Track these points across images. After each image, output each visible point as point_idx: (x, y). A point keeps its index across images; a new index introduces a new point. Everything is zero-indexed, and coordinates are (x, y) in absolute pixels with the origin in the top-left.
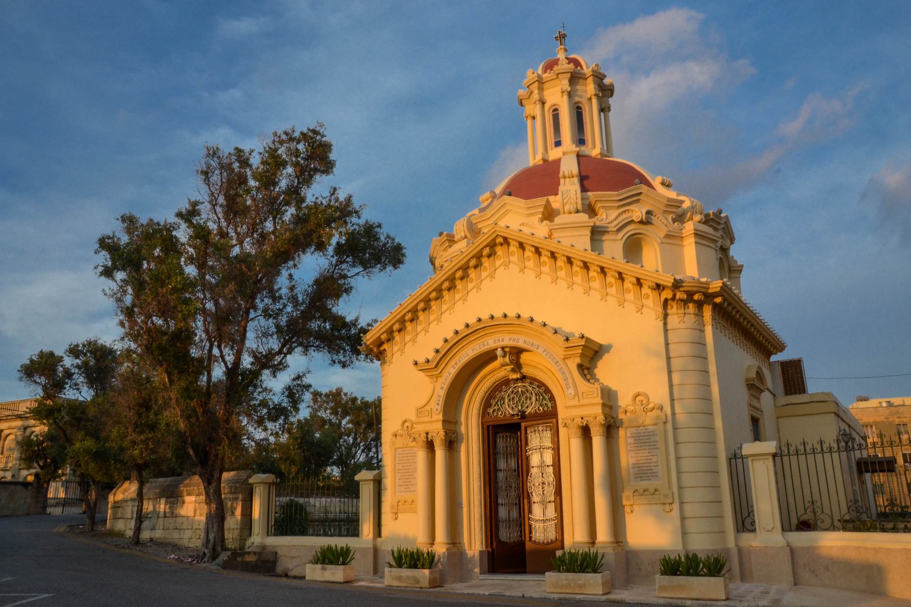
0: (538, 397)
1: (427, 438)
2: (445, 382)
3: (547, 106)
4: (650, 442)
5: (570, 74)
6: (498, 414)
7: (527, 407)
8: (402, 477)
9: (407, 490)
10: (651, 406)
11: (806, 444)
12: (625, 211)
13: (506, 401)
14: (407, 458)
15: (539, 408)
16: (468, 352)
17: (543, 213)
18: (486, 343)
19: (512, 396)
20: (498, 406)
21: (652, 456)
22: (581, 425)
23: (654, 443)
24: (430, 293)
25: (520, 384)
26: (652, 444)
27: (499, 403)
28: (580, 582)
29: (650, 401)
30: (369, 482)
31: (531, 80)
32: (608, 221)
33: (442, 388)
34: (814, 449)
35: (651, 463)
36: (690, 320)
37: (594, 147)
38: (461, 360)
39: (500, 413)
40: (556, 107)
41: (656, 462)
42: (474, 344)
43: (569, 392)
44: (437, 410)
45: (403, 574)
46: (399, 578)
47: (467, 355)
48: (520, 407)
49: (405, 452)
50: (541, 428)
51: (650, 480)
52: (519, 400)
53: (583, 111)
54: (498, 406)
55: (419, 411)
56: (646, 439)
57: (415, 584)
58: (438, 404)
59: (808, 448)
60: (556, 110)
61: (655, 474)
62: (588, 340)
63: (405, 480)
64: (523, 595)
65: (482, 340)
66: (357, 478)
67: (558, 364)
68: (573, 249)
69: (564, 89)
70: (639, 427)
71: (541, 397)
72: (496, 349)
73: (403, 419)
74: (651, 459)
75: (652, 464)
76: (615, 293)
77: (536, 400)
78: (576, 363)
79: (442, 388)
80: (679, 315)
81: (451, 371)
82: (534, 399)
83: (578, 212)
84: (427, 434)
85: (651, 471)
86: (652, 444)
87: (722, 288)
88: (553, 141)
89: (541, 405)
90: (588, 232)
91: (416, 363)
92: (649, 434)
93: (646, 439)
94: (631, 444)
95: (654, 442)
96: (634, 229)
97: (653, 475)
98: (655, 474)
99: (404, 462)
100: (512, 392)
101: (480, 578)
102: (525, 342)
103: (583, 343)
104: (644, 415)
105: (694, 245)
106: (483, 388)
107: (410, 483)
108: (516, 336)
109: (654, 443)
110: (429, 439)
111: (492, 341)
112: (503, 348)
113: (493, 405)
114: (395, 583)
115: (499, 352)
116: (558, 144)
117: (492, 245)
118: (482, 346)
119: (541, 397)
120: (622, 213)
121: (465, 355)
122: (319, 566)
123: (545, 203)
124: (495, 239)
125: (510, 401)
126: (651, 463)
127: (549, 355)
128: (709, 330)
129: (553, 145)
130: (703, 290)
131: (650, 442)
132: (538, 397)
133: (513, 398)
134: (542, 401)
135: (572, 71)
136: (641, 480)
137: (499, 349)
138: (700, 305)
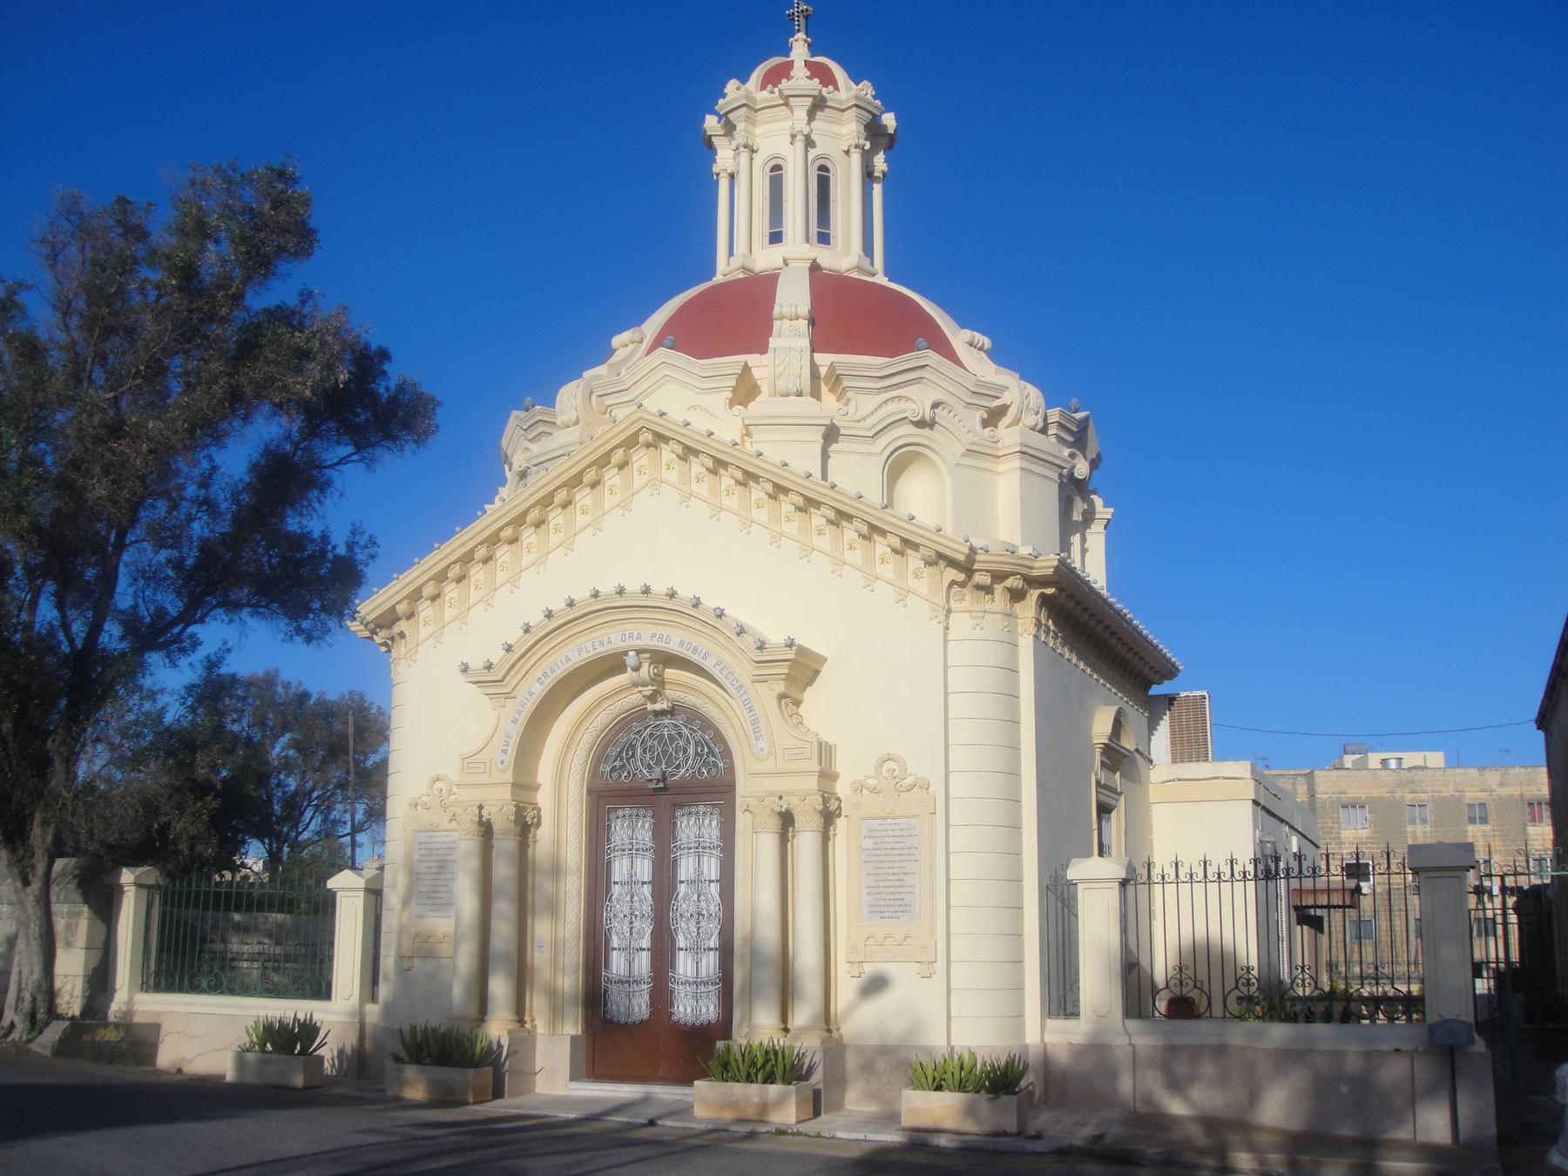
1: (481, 816)
2: (521, 708)
3: (759, 159)
5: (811, 99)
6: (620, 776)
7: (678, 767)
10: (910, 780)
11: (1180, 864)
12: (892, 399)
16: (569, 654)
17: (735, 390)
18: (605, 639)
19: (649, 744)
21: (905, 874)
22: (777, 809)
23: (913, 851)
24: (501, 529)
25: (667, 721)
26: (906, 851)
29: (909, 772)
31: (734, 100)
32: (858, 417)
33: (515, 721)
36: (994, 623)
37: (847, 251)
38: (555, 668)
39: (625, 774)
40: (779, 162)
41: (911, 886)
42: (586, 638)
43: (759, 747)
44: (502, 762)
47: (568, 660)
48: (664, 766)
51: (898, 918)
52: (664, 752)
53: (831, 175)
54: (622, 760)
55: (468, 761)
58: (505, 752)
60: (777, 168)
61: (909, 908)
62: (802, 651)
66: (332, 883)
67: (741, 692)
68: (785, 471)
69: (798, 128)
70: (885, 818)
71: (706, 750)
72: (626, 653)
75: (904, 890)
77: (697, 754)
78: (777, 692)
79: (515, 721)
80: (974, 614)
81: (534, 688)
82: (691, 751)
83: (800, 394)
84: (481, 808)
86: (906, 851)
87: (1056, 568)
88: (767, 231)
89: (705, 764)
90: (817, 436)
91: (465, 669)
92: (903, 833)
94: (868, 849)
95: (909, 848)
96: (908, 435)
97: (904, 909)
98: (909, 908)
100: (651, 735)
102: (682, 644)
103: (792, 657)
104: (896, 797)
105: (1016, 476)
106: (595, 724)
107: (441, 901)
108: (665, 631)
109: (913, 851)
110: (484, 819)
112: (639, 652)
113: (613, 758)
115: (631, 659)
116: (776, 238)
117: (631, 442)
119: (706, 750)
120: (886, 402)
121: (563, 659)
123: (739, 372)
124: (636, 434)
125: (645, 752)
126: (901, 887)
127: (726, 672)
128: (1026, 644)
129: (767, 239)
130: (1024, 571)
134: (708, 756)
135: (816, 93)
136: (882, 918)
137: (631, 654)
138: (1017, 596)
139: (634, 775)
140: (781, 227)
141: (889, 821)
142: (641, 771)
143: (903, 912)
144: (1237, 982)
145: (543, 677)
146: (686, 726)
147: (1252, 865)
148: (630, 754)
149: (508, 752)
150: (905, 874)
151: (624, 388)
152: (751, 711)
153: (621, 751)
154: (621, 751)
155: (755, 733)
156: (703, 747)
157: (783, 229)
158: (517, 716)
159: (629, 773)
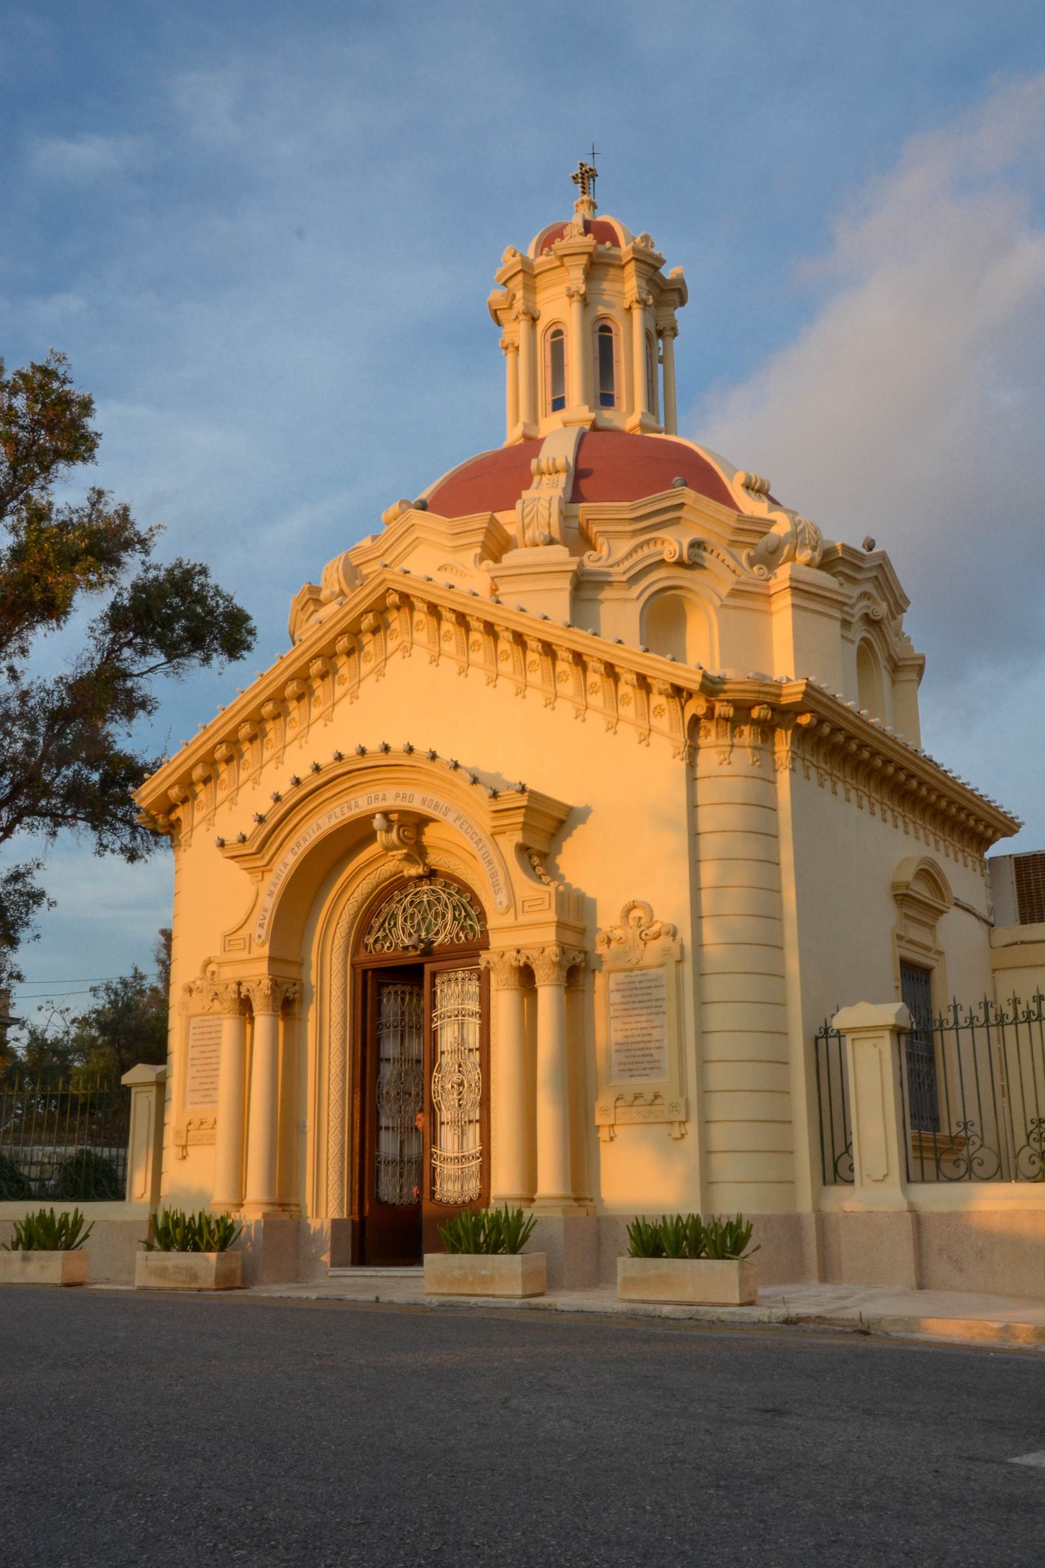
0: (457, 913)
1: (240, 993)
2: (276, 881)
3: (541, 325)
4: (650, 1001)
5: (586, 257)
6: (383, 947)
7: (437, 933)
8: (200, 1074)
9: (206, 1099)
10: (655, 928)
12: (648, 542)
13: (400, 920)
14: (209, 1036)
15: (458, 934)
16: (320, 822)
17: (484, 546)
18: (353, 803)
19: (410, 911)
20: (384, 930)
21: (653, 1027)
22: (515, 964)
23: (659, 1003)
24: (262, 705)
25: (426, 888)
26: (654, 1004)
27: (387, 924)
28: (484, 1272)
29: (655, 919)
30: (148, 1088)
32: (611, 562)
33: (270, 894)
34: (972, 1018)
35: (650, 1042)
36: (743, 758)
37: (631, 409)
38: (307, 837)
39: (388, 944)
40: (560, 327)
41: (659, 1041)
42: (333, 806)
43: (498, 900)
44: (260, 937)
45: (170, 1264)
46: (162, 1272)
47: (319, 827)
48: (423, 934)
49: (207, 1023)
50: (460, 975)
51: (647, 1075)
52: (424, 919)
53: (613, 335)
54: (384, 930)
55: (229, 939)
56: (644, 995)
57: (190, 1283)
58: (261, 926)
59: (962, 1016)
60: (558, 333)
61: (657, 1064)
62: (534, 796)
63: (204, 1080)
64: (377, 1298)
65: (345, 799)
66: (126, 1079)
67: (481, 845)
68: (522, 616)
69: (574, 289)
70: (631, 970)
71: (463, 914)
72: (373, 816)
73: (203, 958)
74: (650, 1035)
75: (652, 1045)
76: (602, 705)
77: (455, 918)
78: (514, 844)
79: (270, 894)
80: (719, 749)
81: (289, 860)
82: (449, 916)
83: (551, 542)
84: (239, 984)
85: (648, 1059)
86: (654, 1004)
87: (805, 693)
88: (550, 399)
89: (462, 928)
90: (565, 584)
91: (222, 844)
92: (649, 984)
93: (644, 995)
94: (616, 1004)
95: (657, 1000)
96: (667, 578)
97: (652, 1065)
98: (657, 1064)
99: (203, 1043)
100: (412, 902)
101: (330, 1273)
102: (424, 801)
103: (525, 803)
104: (642, 946)
105: (788, 613)
106: (356, 894)
108: (408, 790)
109: (659, 1003)
110: (242, 995)
111: (365, 798)
112: (386, 814)
113: (375, 929)
114: (154, 1282)
115: (378, 822)
116: (559, 404)
117: (380, 610)
118: (345, 809)
119: (463, 914)
120: (640, 546)
121: (315, 827)
122: (19, 1253)
123: (486, 525)
124: (383, 597)
125: (405, 920)
126: (650, 1042)
127: (465, 826)
128: (784, 777)
129: (550, 407)
130: (768, 699)
131: (650, 1001)
132: (457, 913)
133: (412, 915)
135: (590, 250)
136: (631, 1076)
137: (378, 816)
138: (766, 730)
139: (397, 944)
140: (563, 392)
141: (636, 972)
142: (402, 940)
143: (652, 1068)
144: (1028, 1137)
145: (296, 848)
146: (444, 892)
148: (392, 923)
149: (265, 926)
150: (653, 1027)
151: (378, 554)
152: (490, 864)
153: (384, 922)
154: (384, 922)
155: (494, 886)
156: (460, 911)
157: (565, 395)
158: (272, 888)
159: (391, 943)
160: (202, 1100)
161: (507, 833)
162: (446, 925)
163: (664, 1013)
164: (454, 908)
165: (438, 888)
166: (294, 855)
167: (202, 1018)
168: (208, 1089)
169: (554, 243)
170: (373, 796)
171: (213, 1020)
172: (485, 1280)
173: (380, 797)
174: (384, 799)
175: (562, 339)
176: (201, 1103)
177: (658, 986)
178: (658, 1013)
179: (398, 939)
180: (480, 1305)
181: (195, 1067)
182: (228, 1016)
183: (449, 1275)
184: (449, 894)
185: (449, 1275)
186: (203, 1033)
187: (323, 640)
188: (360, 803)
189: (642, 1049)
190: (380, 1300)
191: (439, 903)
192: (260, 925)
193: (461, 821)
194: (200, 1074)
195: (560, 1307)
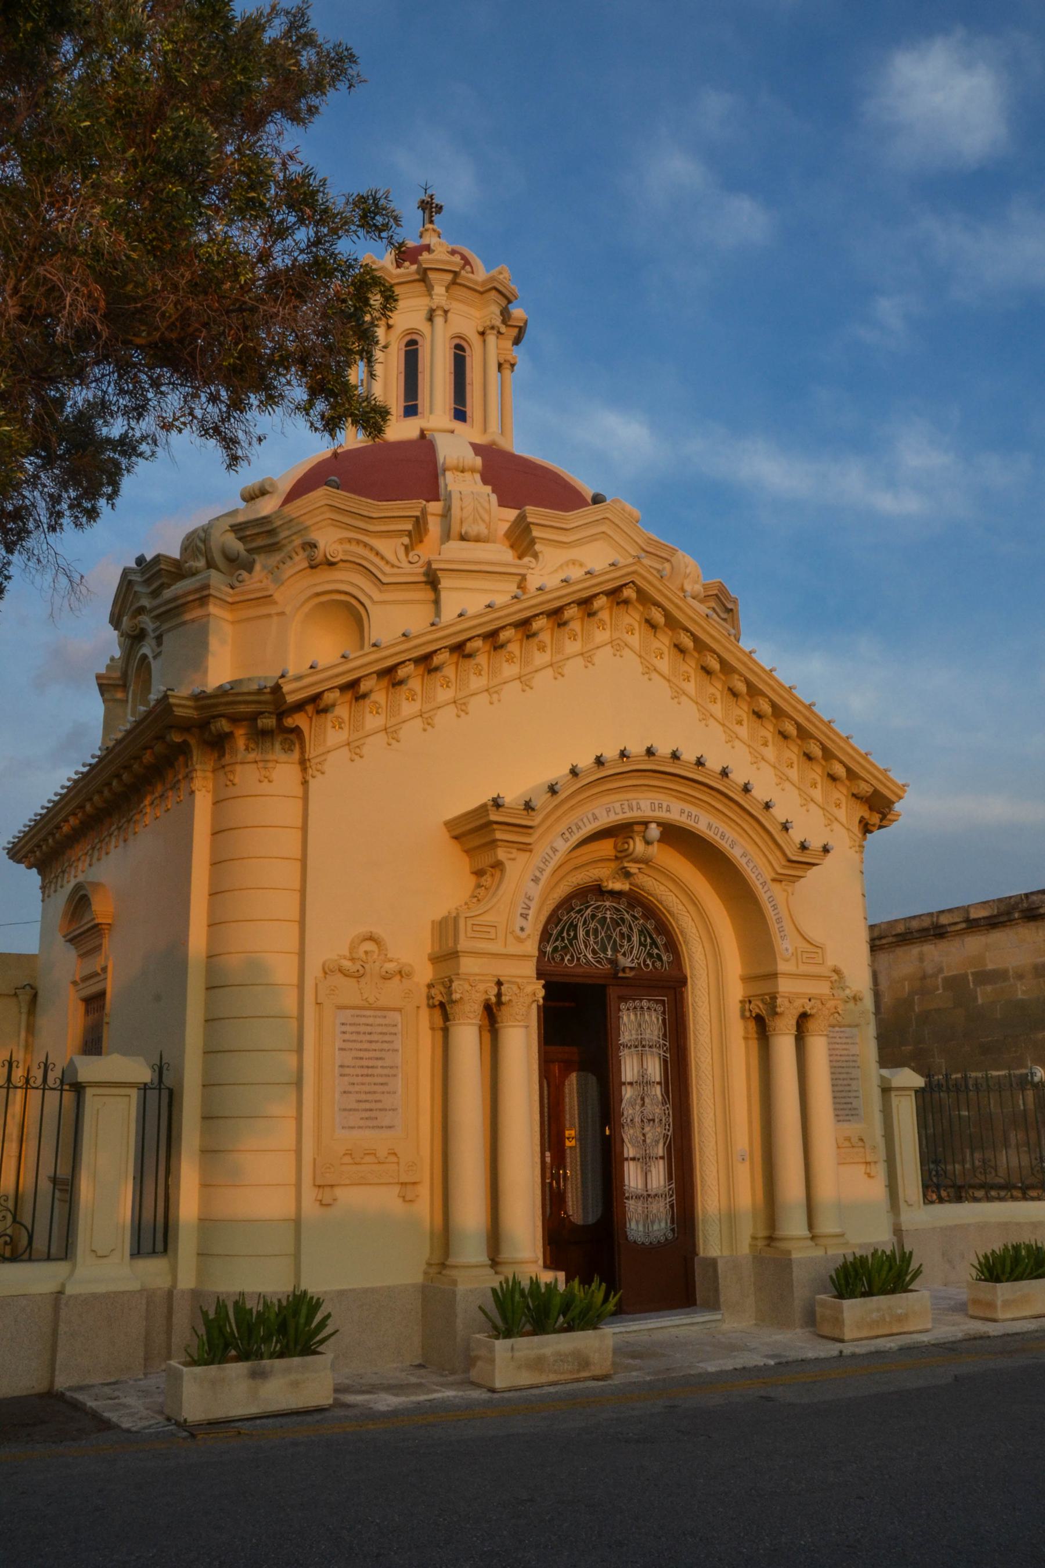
0: (643, 939)
4: (848, 1055)
6: (563, 959)
8: (357, 1088)
9: (369, 1123)
13: (581, 933)
14: (368, 1037)
15: (645, 961)
16: (596, 811)
20: (563, 939)
21: (851, 1079)
23: (855, 1058)
27: (565, 934)
28: (899, 1311)
30: (127, 1091)
31: (437, 261)
35: (850, 1091)
39: (568, 957)
40: (415, 337)
43: (784, 946)
45: (548, 1351)
46: (537, 1364)
47: (595, 818)
49: (363, 1020)
50: (645, 1003)
51: (849, 1121)
56: (843, 1049)
57: (579, 1371)
60: (412, 343)
63: (364, 1097)
64: (841, 1352)
65: (630, 796)
67: (766, 889)
71: (648, 940)
73: (378, 931)
74: (849, 1085)
75: (851, 1094)
77: (641, 944)
82: (635, 939)
85: (849, 1106)
86: (851, 1058)
93: (843, 1049)
97: (853, 1113)
99: (359, 1046)
100: (593, 917)
107: (379, 1106)
109: (855, 1058)
111: (648, 802)
114: (525, 1378)
118: (626, 809)
119: (648, 940)
121: (590, 816)
122: (237, 1369)
125: (587, 933)
126: (850, 1091)
127: (751, 865)
131: (848, 1055)
132: (643, 939)
133: (596, 931)
134: (651, 947)
137: (653, 826)
139: (578, 959)
140: (417, 400)
141: (837, 1029)
142: (585, 955)
143: (852, 1115)
145: (567, 833)
146: (628, 912)
147: (42, 1070)
148: (572, 934)
149: (530, 918)
150: (851, 1079)
151: (564, 526)
152: (775, 909)
153: (562, 932)
154: (562, 932)
155: (780, 932)
156: (645, 937)
157: (419, 402)
158: (538, 874)
159: (572, 956)
160: (362, 1123)
161: (784, 883)
162: (633, 948)
163: (858, 1067)
164: (641, 932)
165: (621, 907)
166: (566, 841)
167: (358, 1012)
168: (371, 1110)
169: (421, 255)
170: (657, 802)
171: (375, 1017)
172: (900, 1319)
173: (665, 806)
174: (668, 810)
175: (417, 349)
176: (360, 1127)
177: (853, 1044)
178: (854, 1067)
179: (580, 954)
180: (933, 1342)
181: (346, 1078)
182: (474, 1021)
183: (868, 1319)
184: (634, 916)
185: (868, 1319)
186: (358, 1033)
187: (561, 600)
188: (643, 807)
189: (844, 1097)
190: (844, 1354)
191: (624, 923)
192: (521, 915)
193: (747, 858)
194: (357, 1088)
195: (992, 1333)
